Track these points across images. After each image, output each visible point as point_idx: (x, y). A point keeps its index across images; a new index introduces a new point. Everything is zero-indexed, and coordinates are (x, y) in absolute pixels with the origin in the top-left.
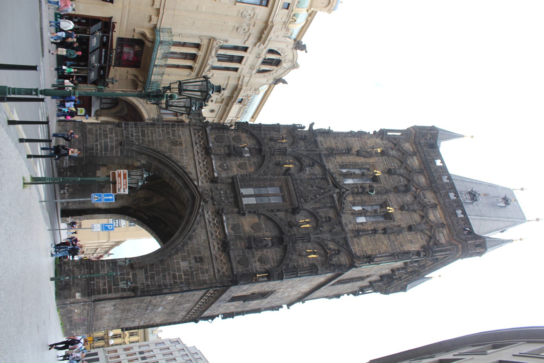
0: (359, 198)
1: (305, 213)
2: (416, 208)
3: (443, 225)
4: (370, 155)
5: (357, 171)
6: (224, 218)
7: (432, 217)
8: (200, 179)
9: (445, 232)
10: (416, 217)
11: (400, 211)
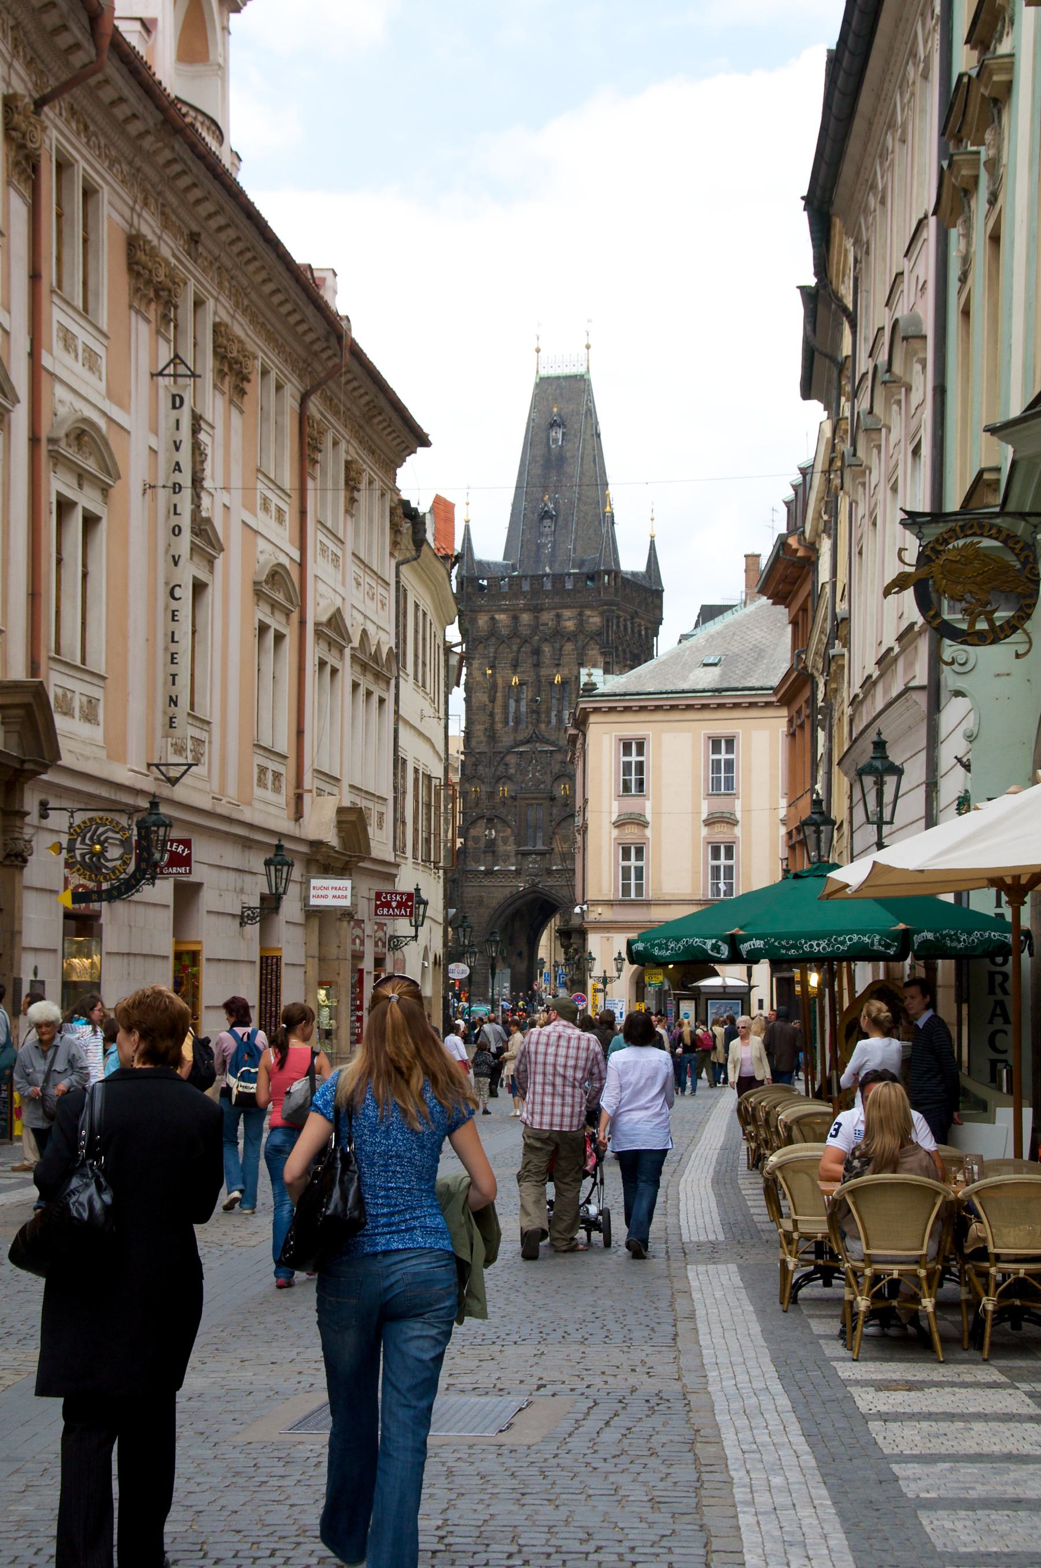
0: (543, 716)
1: (555, 785)
2: (557, 645)
3: (581, 614)
4: (494, 686)
5: (512, 704)
6: (554, 868)
7: (570, 625)
8: (516, 883)
9: (588, 613)
10: (569, 647)
11: (561, 668)
